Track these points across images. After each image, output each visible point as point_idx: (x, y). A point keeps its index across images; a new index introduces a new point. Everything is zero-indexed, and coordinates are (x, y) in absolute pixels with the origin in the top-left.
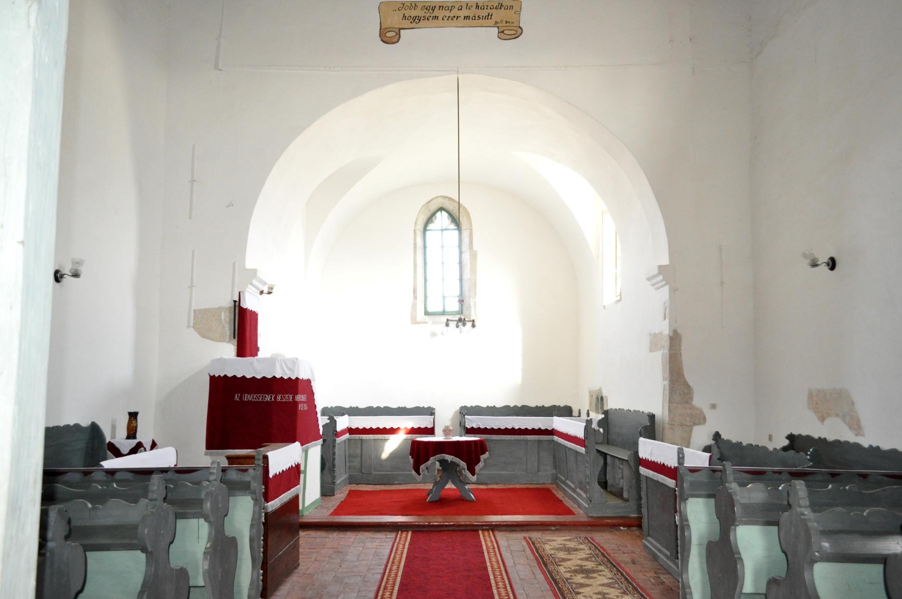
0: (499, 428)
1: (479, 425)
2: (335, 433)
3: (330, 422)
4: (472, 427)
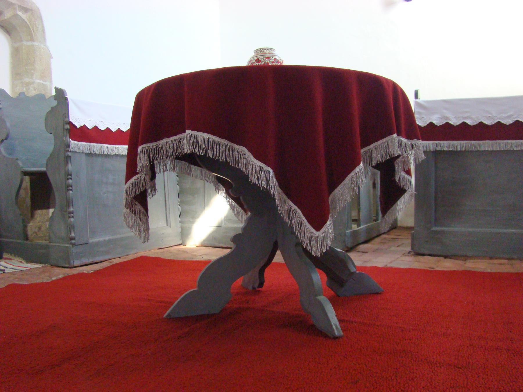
0: (499, 123)
1: (447, 118)
2: (68, 127)
3: (58, 103)
4: (431, 124)
